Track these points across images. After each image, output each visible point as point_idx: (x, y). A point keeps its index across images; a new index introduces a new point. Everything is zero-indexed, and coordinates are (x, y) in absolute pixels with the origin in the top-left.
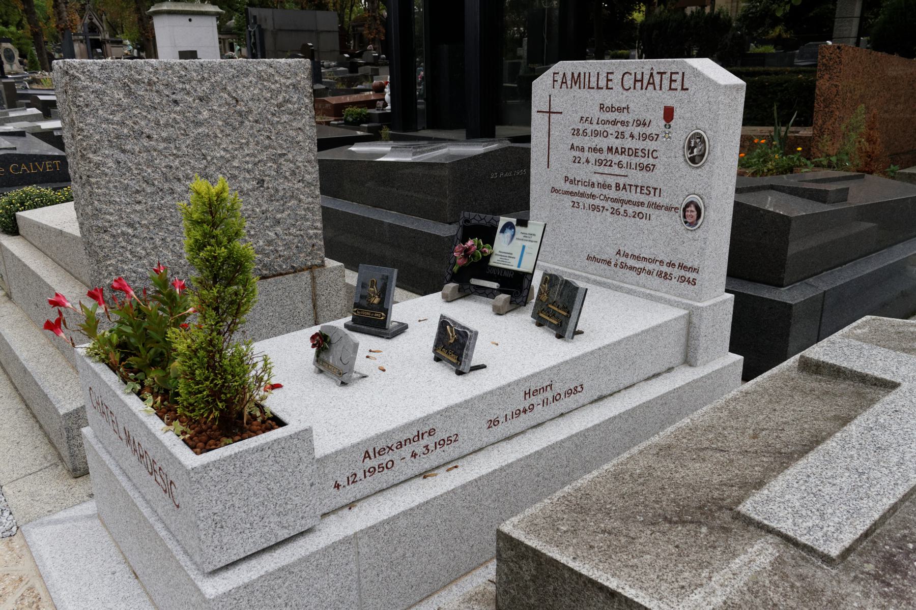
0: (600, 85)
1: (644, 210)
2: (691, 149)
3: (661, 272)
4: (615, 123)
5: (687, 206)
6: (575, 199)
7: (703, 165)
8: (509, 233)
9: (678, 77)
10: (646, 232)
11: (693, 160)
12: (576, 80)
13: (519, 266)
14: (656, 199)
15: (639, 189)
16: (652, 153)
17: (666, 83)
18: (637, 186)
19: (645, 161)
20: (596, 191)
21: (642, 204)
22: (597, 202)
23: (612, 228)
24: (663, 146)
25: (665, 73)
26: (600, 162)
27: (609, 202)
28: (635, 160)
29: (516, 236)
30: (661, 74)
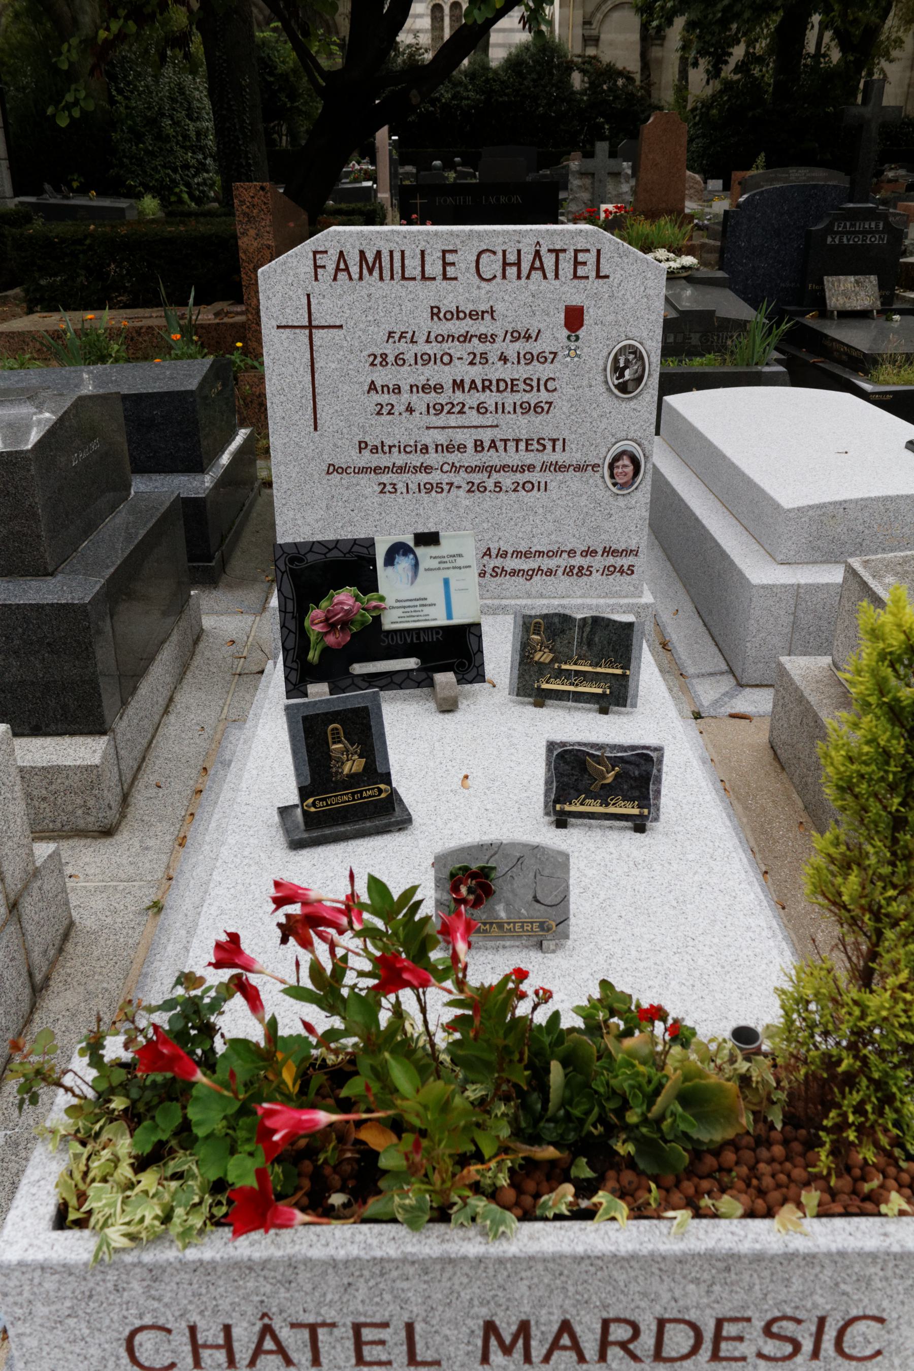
0: (429, 271)
1: (535, 477)
2: (619, 371)
3: (572, 568)
4: (466, 338)
5: (616, 459)
6: (385, 478)
7: (640, 394)
8: (404, 563)
9: (591, 258)
10: (541, 511)
11: (623, 388)
12: (371, 264)
13: (449, 616)
14: (559, 457)
15: (522, 446)
16: (546, 384)
17: (566, 267)
18: (517, 441)
19: (532, 398)
20: (432, 458)
21: (531, 468)
22: (435, 477)
23: (472, 516)
24: (567, 371)
25: (564, 251)
26: (439, 409)
27: (462, 473)
28: (510, 399)
29: (422, 567)
30: (557, 252)
